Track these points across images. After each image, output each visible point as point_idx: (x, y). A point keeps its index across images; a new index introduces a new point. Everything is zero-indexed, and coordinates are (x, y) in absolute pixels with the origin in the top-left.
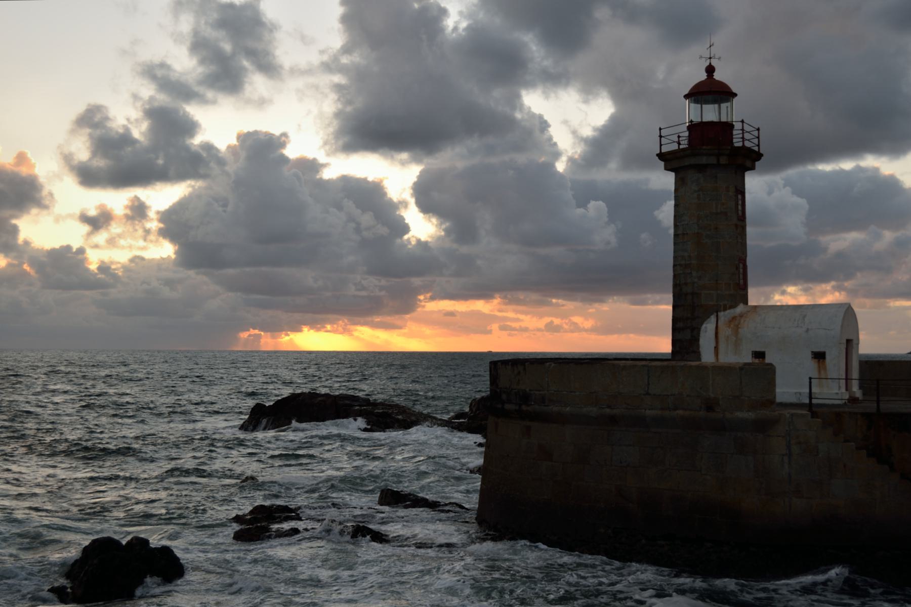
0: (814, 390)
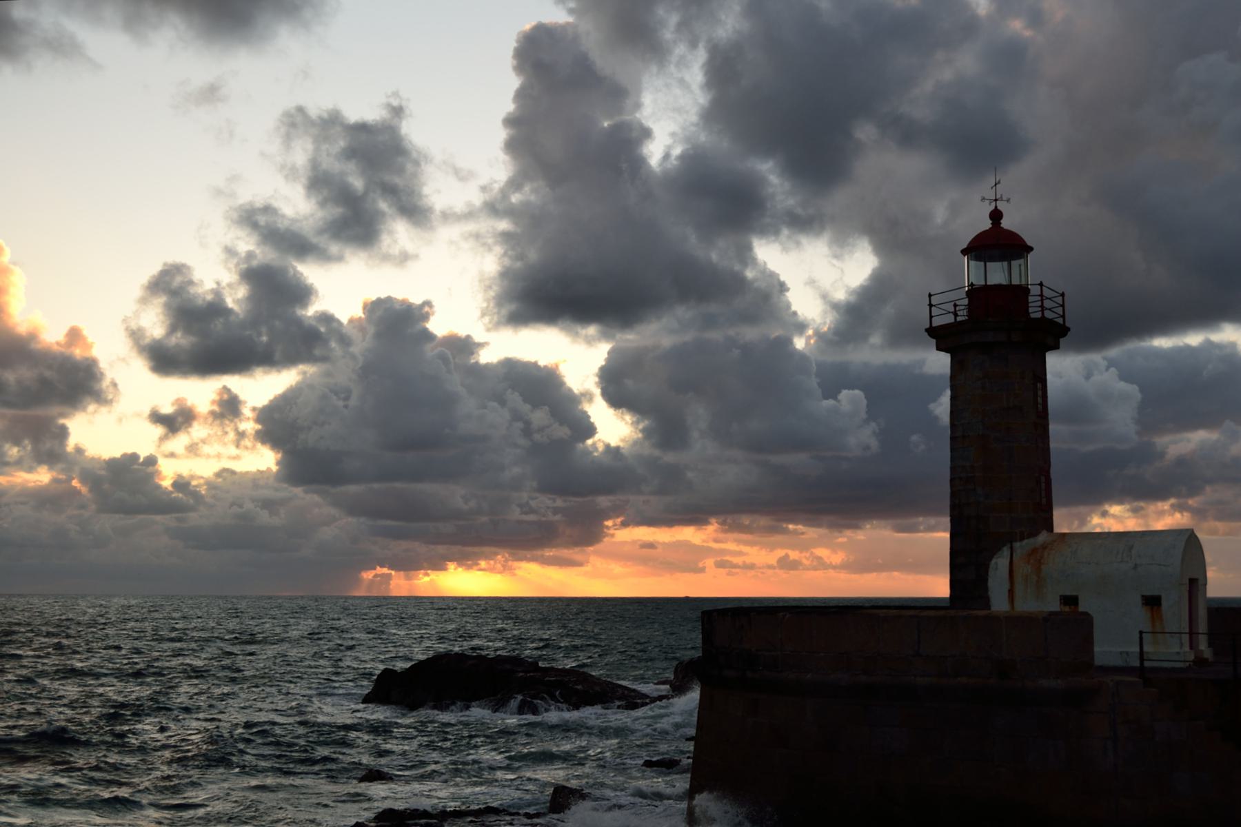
0: (1146, 649)
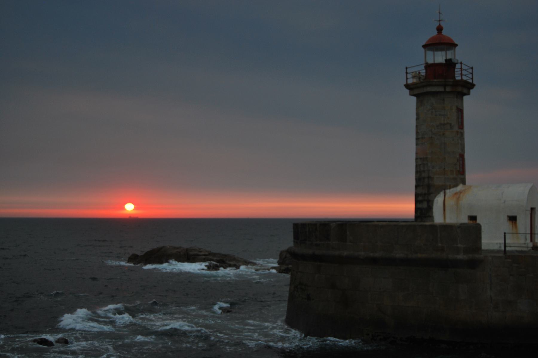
0: (507, 242)
